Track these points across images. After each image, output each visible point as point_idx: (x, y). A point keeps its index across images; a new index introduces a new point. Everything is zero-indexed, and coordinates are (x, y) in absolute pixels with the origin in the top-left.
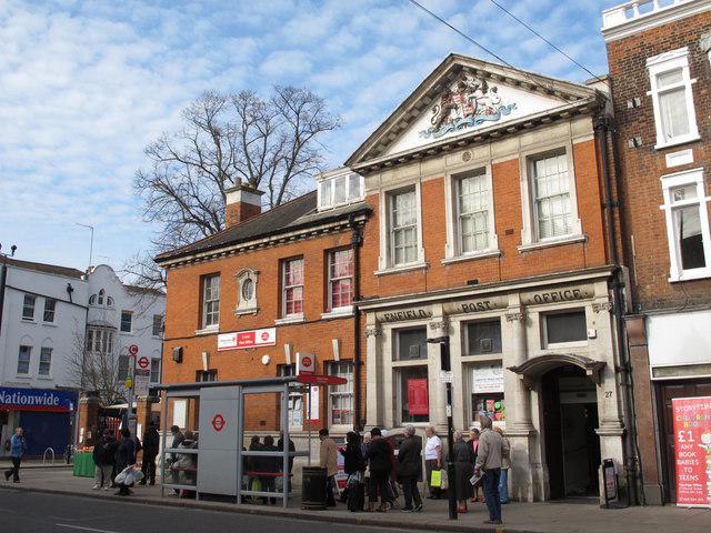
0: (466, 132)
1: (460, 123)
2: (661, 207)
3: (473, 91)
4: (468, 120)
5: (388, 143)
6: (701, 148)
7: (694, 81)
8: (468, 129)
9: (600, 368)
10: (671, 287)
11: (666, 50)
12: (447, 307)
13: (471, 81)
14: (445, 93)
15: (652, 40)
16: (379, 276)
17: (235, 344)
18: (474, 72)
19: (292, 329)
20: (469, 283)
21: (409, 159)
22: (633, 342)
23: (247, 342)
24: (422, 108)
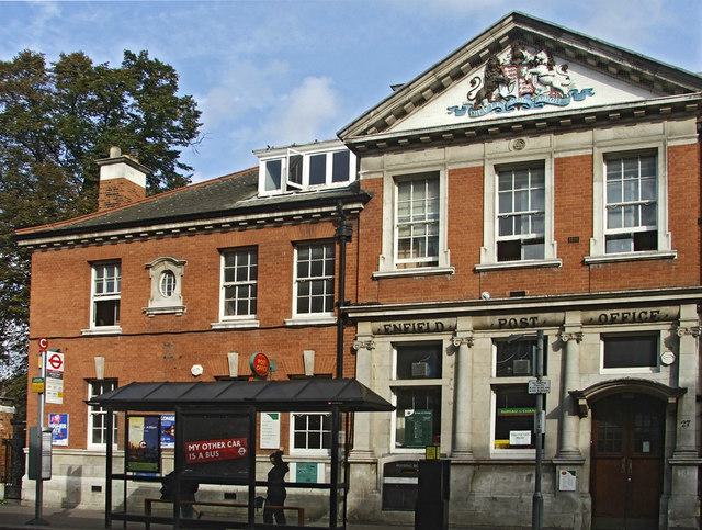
1: (512, 102)
4: (523, 100)
5: (402, 114)
8: (521, 112)
16: (378, 278)
20: (512, 294)
21: (438, 138)
24: (458, 75)
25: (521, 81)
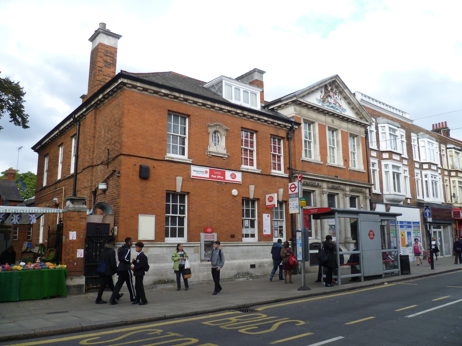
0: (331, 110)
17: (207, 176)
19: (252, 176)
20: (336, 176)
23: (218, 177)
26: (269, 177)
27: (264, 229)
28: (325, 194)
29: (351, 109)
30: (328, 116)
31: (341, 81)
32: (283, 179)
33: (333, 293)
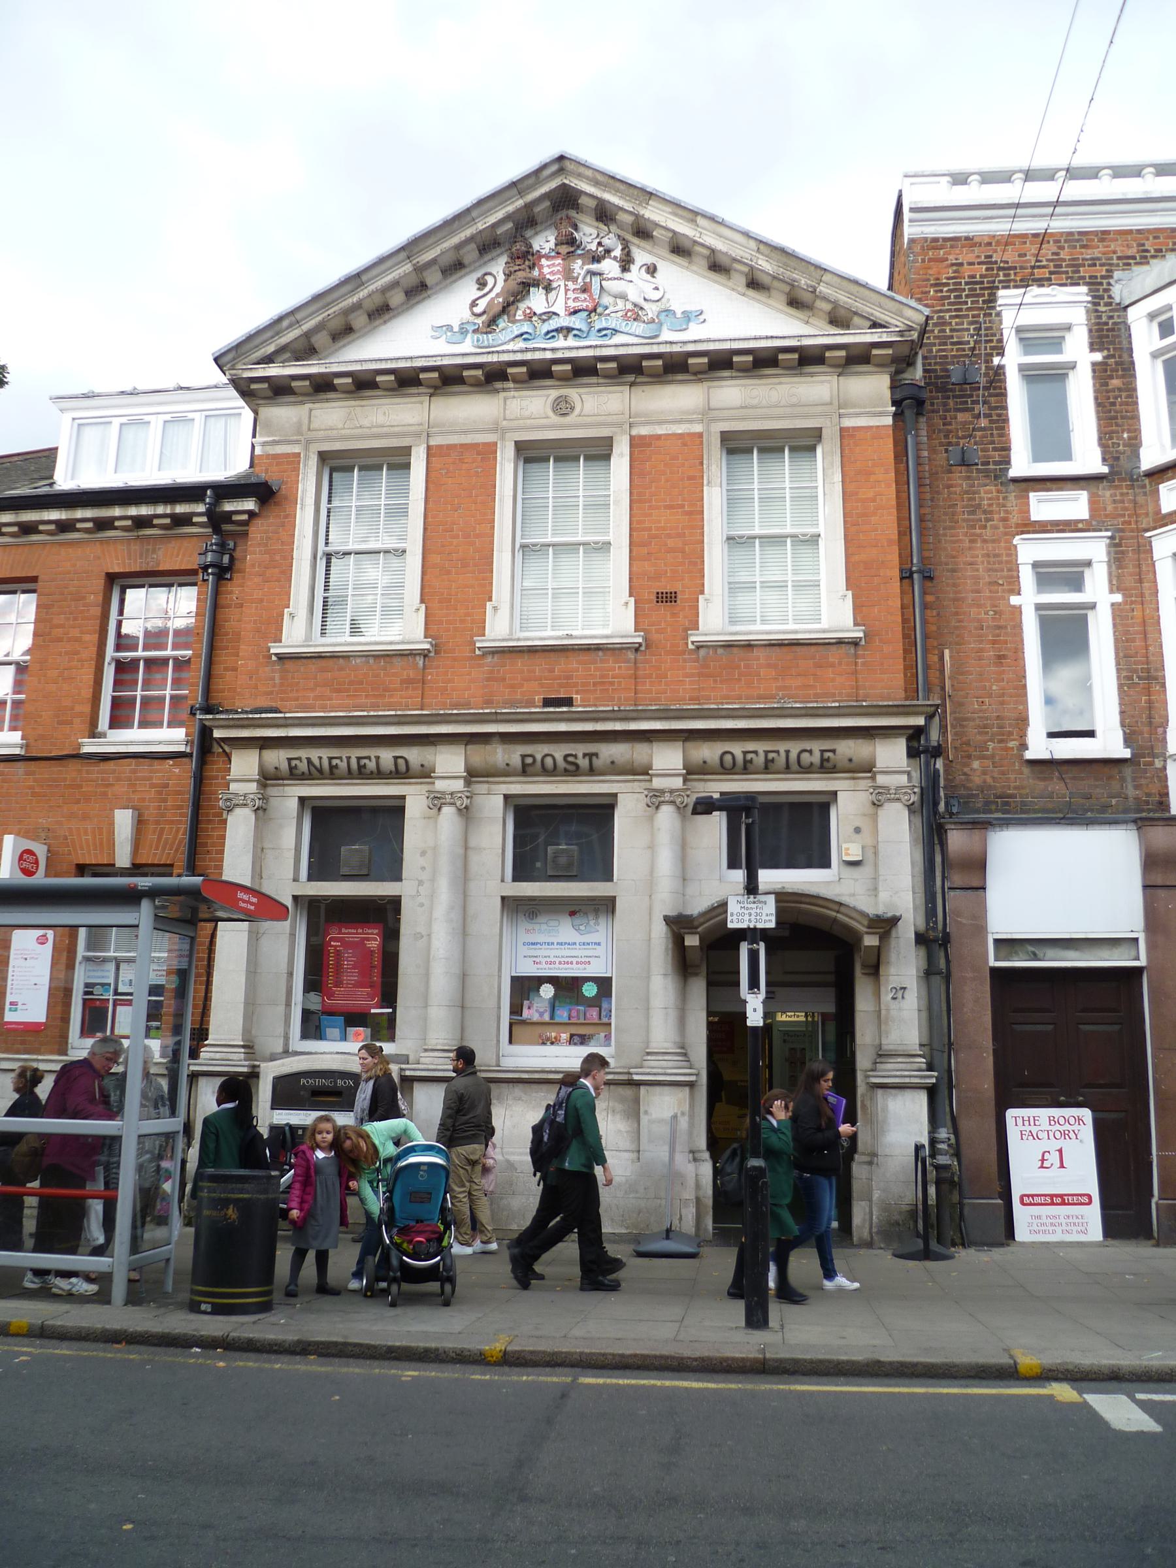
0: (566, 347)
1: (554, 324)
2: (1014, 600)
3: (597, 259)
4: (577, 322)
5: (344, 332)
6: (1106, 493)
7: (1098, 357)
8: (571, 342)
9: (886, 925)
10: (1026, 770)
11: (1041, 282)
12: (482, 755)
13: (589, 234)
14: (519, 247)
15: (1011, 256)
16: (281, 657)
18: (604, 214)
20: (547, 702)
22: (957, 879)
24: (454, 268)
25: (571, 285)
26: (73, 766)
27: (9, 998)
28: (448, 811)
29: (751, 292)
30: (516, 389)
31: (599, 177)
32: (156, 762)
33: (276, 1352)
